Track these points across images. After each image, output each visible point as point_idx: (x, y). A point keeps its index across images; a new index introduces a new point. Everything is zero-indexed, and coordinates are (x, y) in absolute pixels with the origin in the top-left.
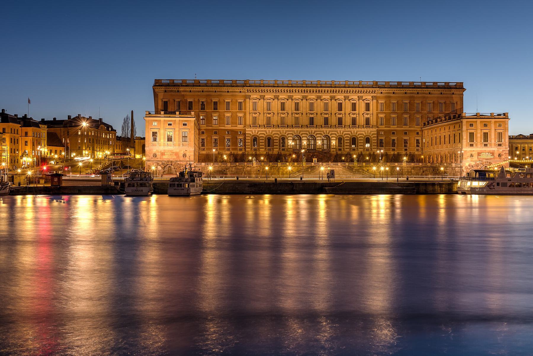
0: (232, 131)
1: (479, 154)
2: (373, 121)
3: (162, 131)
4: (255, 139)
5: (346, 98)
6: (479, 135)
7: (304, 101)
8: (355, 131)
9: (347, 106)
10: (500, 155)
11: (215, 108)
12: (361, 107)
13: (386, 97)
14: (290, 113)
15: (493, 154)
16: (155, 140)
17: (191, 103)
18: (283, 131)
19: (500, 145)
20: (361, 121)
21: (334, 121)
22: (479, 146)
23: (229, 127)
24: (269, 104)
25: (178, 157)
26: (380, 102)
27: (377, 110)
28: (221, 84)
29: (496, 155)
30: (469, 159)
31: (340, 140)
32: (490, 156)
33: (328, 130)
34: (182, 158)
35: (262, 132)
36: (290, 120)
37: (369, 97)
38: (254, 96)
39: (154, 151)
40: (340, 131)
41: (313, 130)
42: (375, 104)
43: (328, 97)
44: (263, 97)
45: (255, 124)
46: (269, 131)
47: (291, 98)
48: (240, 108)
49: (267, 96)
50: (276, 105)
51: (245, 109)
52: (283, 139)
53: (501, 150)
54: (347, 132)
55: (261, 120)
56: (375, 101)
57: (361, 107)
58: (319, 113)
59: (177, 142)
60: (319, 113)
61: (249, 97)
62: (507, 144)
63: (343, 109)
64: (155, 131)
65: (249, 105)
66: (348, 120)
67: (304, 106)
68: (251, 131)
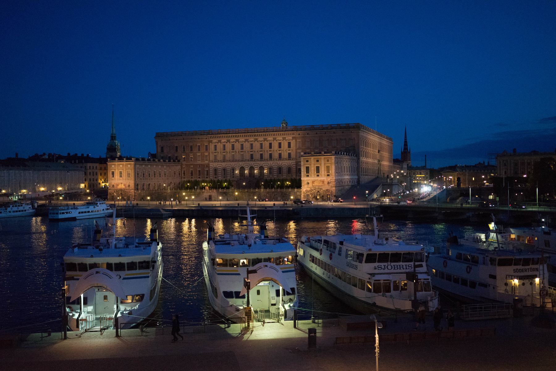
0: (202, 165)
1: (313, 182)
2: (293, 156)
3: (117, 171)
4: (216, 170)
5: (275, 139)
6: (313, 168)
7: (247, 142)
8: (280, 163)
9: (275, 145)
10: (328, 183)
11: (191, 150)
12: (285, 145)
13: (303, 137)
14: (237, 151)
15: (323, 182)
16: (113, 177)
17: (177, 147)
18: (233, 164)
19: (328, 175)
20: (285, 155)
21: (266, 156)
22: (313, 175)
23: (199, 162)
24: (224, 146)
27: (296, 147)
29: (326, 183)
30: (306, 186)
31: (270, 169)
32: (321, 184)
33: (262, 162)
34: (127, 188)
35: (220, 165)
36: (238, 157)
38: (215, 141)
39: (113, 183)
40: (270, 163)
41: (252, 163)
42: (294, 143)
43: (262, 139)
44: (220, 141)
45: (216, 160)
46: (224, 165)
47: (237, 141)
48: (207, 150)
49: (223, 141)
50: (229, 146)
52: (233, 170)
53: (329, 179)
54: (275, 164)
55: (220, 157)
56: (294, 140)
57: (285, 145)
58: (256, 151)
59: (124, 178)
60: (256, 151)
61: (211, 142)
63: (282, 146)
65: (212, 147)
66: (276, 155)
67: (247, 146)
68: (213, 165)
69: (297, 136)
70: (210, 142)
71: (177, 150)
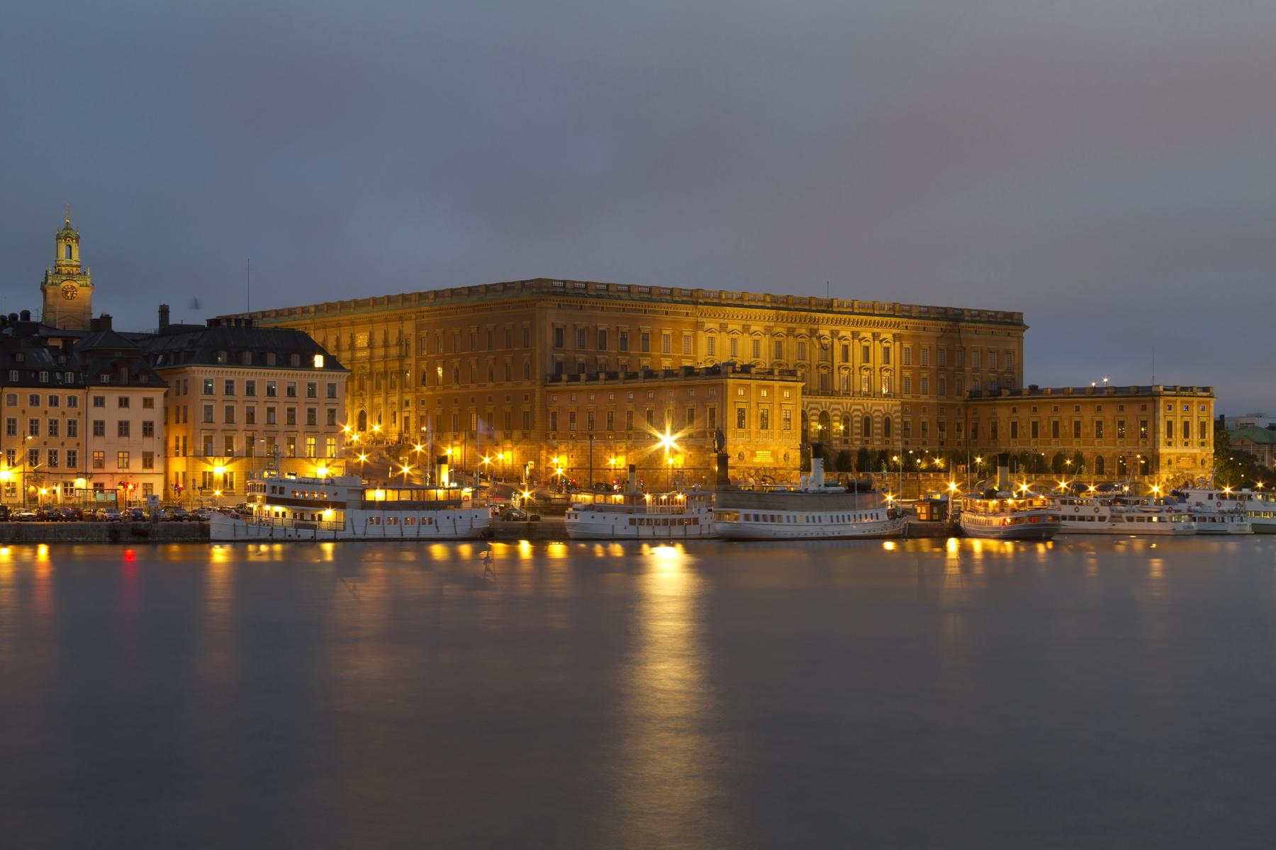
15: (1194, 458)
19: (1203, 444)
25: (777, 460)
26: (906, 345)
28: (652, 296)
29: (1199, 462)
32: (1190, 465)
34: (782, 463)
37: (889, 337)
40: (847, 401)
44: (723, 328)
51: (695, 352)
54: (857, 406)
56: (898, 344)
59: (776, 431)
62: (1212, 442)
64: (742, 406)
69: (904, 332)
70: (698, 326)
71: (603, 346)
